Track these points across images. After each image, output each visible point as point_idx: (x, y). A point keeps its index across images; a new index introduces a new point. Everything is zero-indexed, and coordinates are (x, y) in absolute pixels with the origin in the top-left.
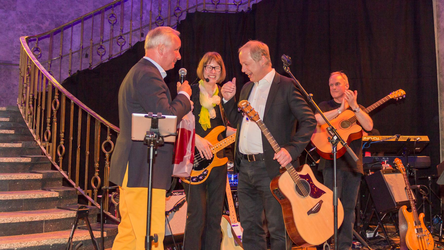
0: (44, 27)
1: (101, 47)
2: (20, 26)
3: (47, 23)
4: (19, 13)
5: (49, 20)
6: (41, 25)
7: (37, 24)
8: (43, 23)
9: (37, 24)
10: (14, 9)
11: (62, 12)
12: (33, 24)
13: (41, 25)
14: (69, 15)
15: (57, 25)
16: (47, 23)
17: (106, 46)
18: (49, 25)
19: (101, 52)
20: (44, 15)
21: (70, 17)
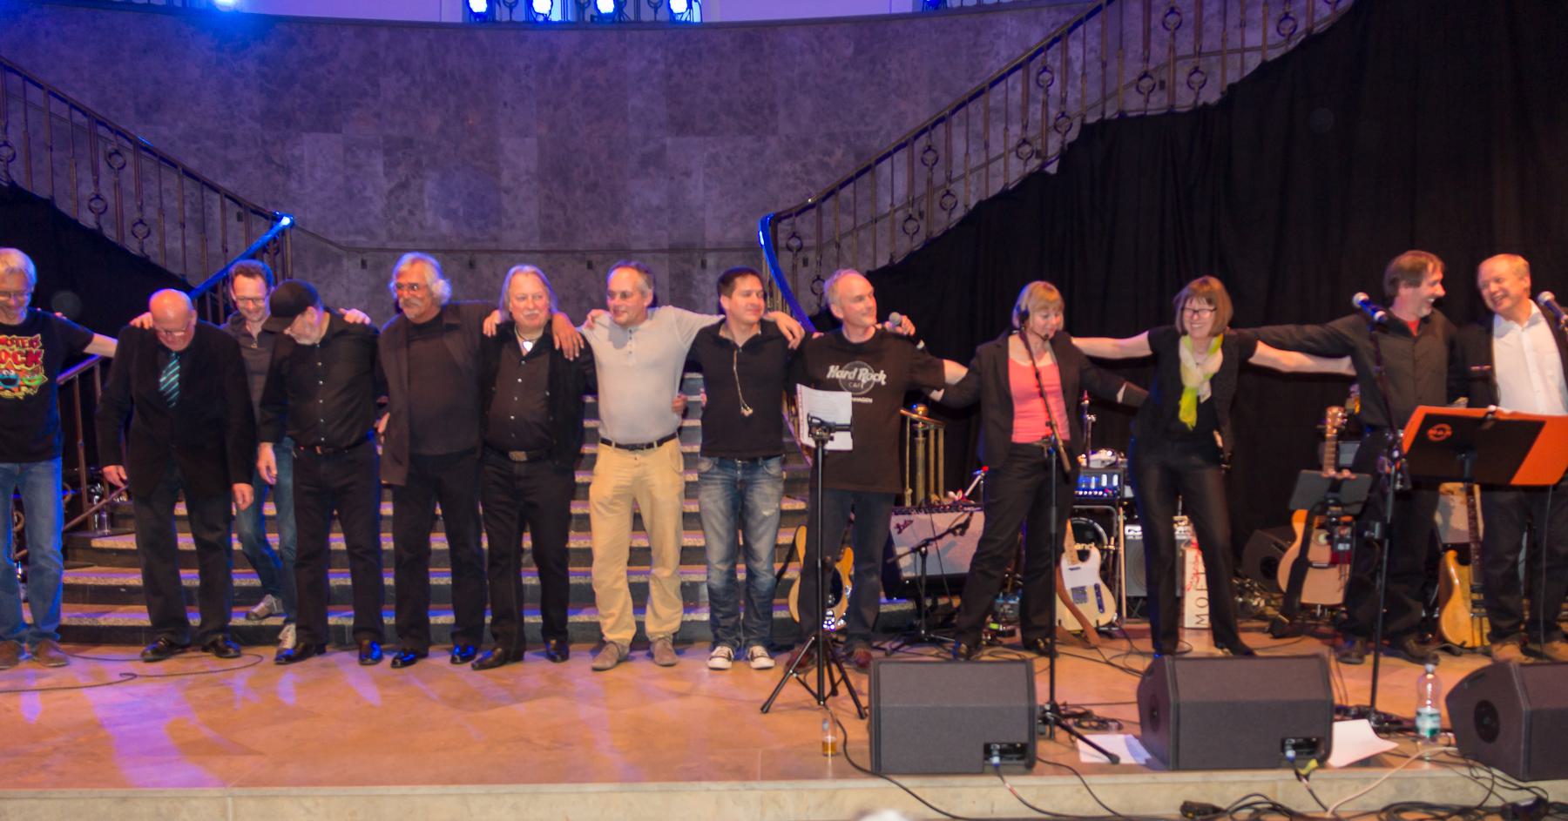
0: (832, 162)
1: (948, 193)
2: (787, 167)
3: (839, 153)
4: (784, 139)
5: (842, 145)
6: (827, 159)
7: (820, 157)
8: (829, 153)
9: (820, 157)
10: (774, 131)
11: (867, 125)
12: (812, 159)
13: (827, 159)
14: (881, 128)
15: (859, 155)
16: (839, 153)
17: (958, 188)
18: (843, 155)
19: (949, 201)
20: (831, 137)
21: (883, 133)
